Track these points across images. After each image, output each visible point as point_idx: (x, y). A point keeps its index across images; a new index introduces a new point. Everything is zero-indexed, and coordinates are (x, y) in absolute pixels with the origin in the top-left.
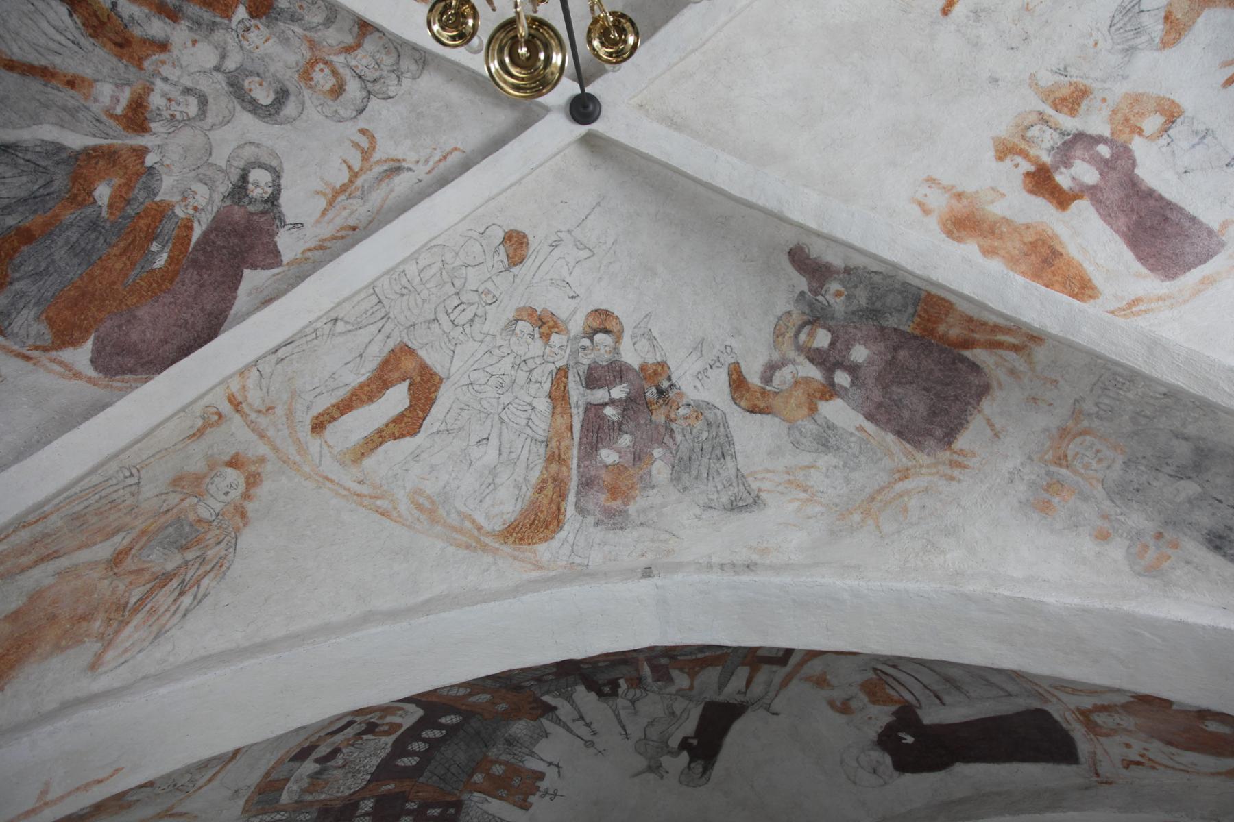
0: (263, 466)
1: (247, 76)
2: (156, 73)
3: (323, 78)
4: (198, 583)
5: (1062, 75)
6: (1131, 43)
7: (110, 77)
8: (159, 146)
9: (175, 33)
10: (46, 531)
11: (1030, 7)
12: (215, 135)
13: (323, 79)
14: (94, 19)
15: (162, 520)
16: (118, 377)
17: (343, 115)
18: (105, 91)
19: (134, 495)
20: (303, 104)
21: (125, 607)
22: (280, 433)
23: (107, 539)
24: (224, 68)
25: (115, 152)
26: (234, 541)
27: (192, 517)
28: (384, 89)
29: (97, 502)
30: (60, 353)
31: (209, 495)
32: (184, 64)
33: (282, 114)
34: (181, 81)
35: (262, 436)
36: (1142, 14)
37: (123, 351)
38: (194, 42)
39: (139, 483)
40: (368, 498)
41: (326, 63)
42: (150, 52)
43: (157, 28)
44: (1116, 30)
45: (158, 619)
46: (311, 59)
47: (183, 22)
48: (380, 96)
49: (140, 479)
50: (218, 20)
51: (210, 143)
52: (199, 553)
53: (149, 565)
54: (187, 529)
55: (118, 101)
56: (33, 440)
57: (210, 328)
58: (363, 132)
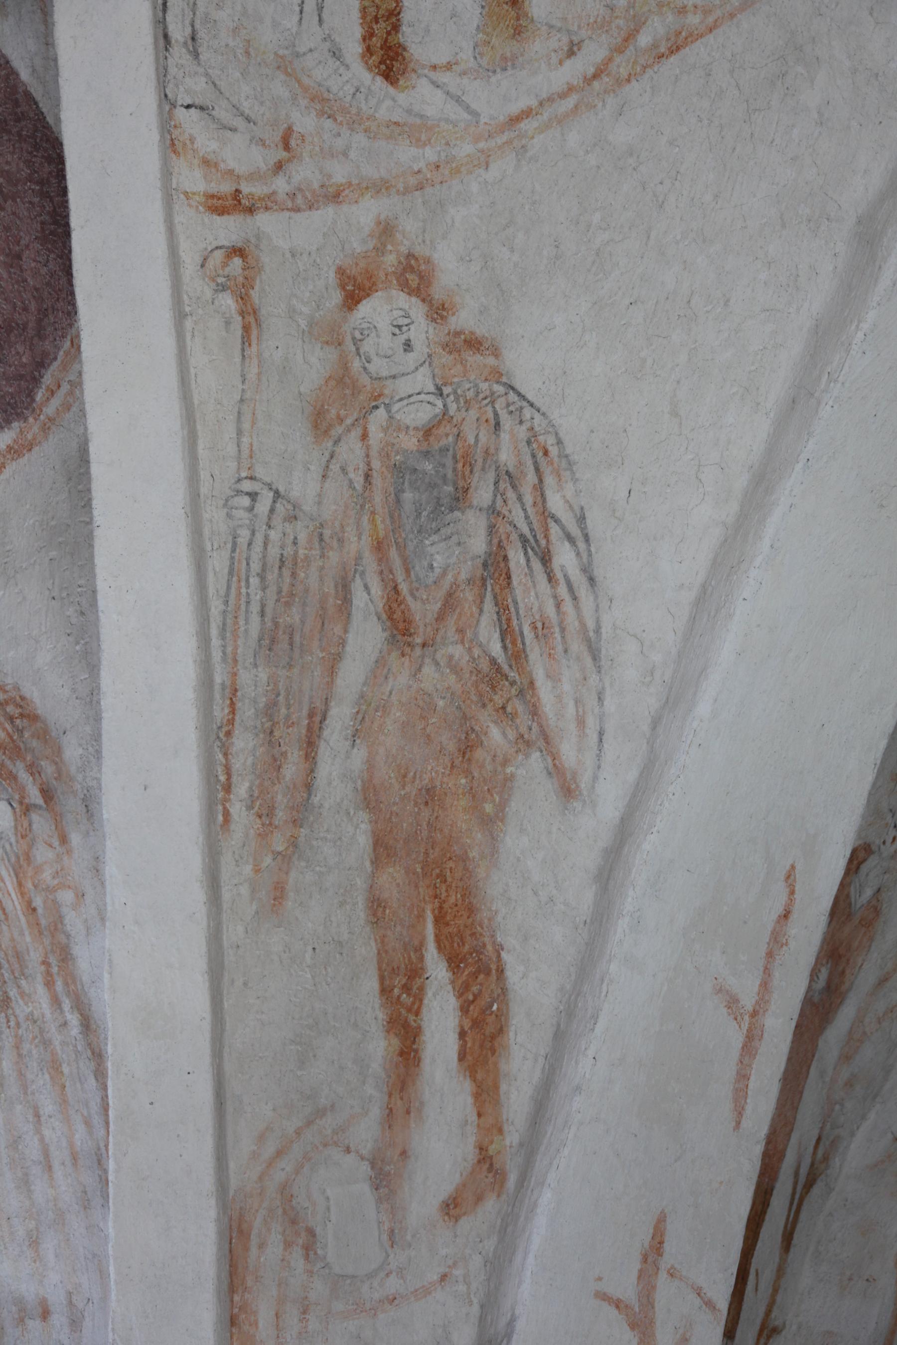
0: (399, 236)
4: (546, 516)
10: (261, 705)
15: (378, 498)
16: (39, 396)
19: (296, 518)
21: (499, 670)
22: (352, 155)
26: (512, 396)
27: (410, 443)
29: (264, 589)
31: (389, 382)
35: (335, 197)
39: (277, 493)
40: (618, 59)
45: (563, 630)
49: (269, 486)
52: (491, 476)
53: (449, 578)
54: (428, 467)
56: (74, 620)
57: (36, 147)
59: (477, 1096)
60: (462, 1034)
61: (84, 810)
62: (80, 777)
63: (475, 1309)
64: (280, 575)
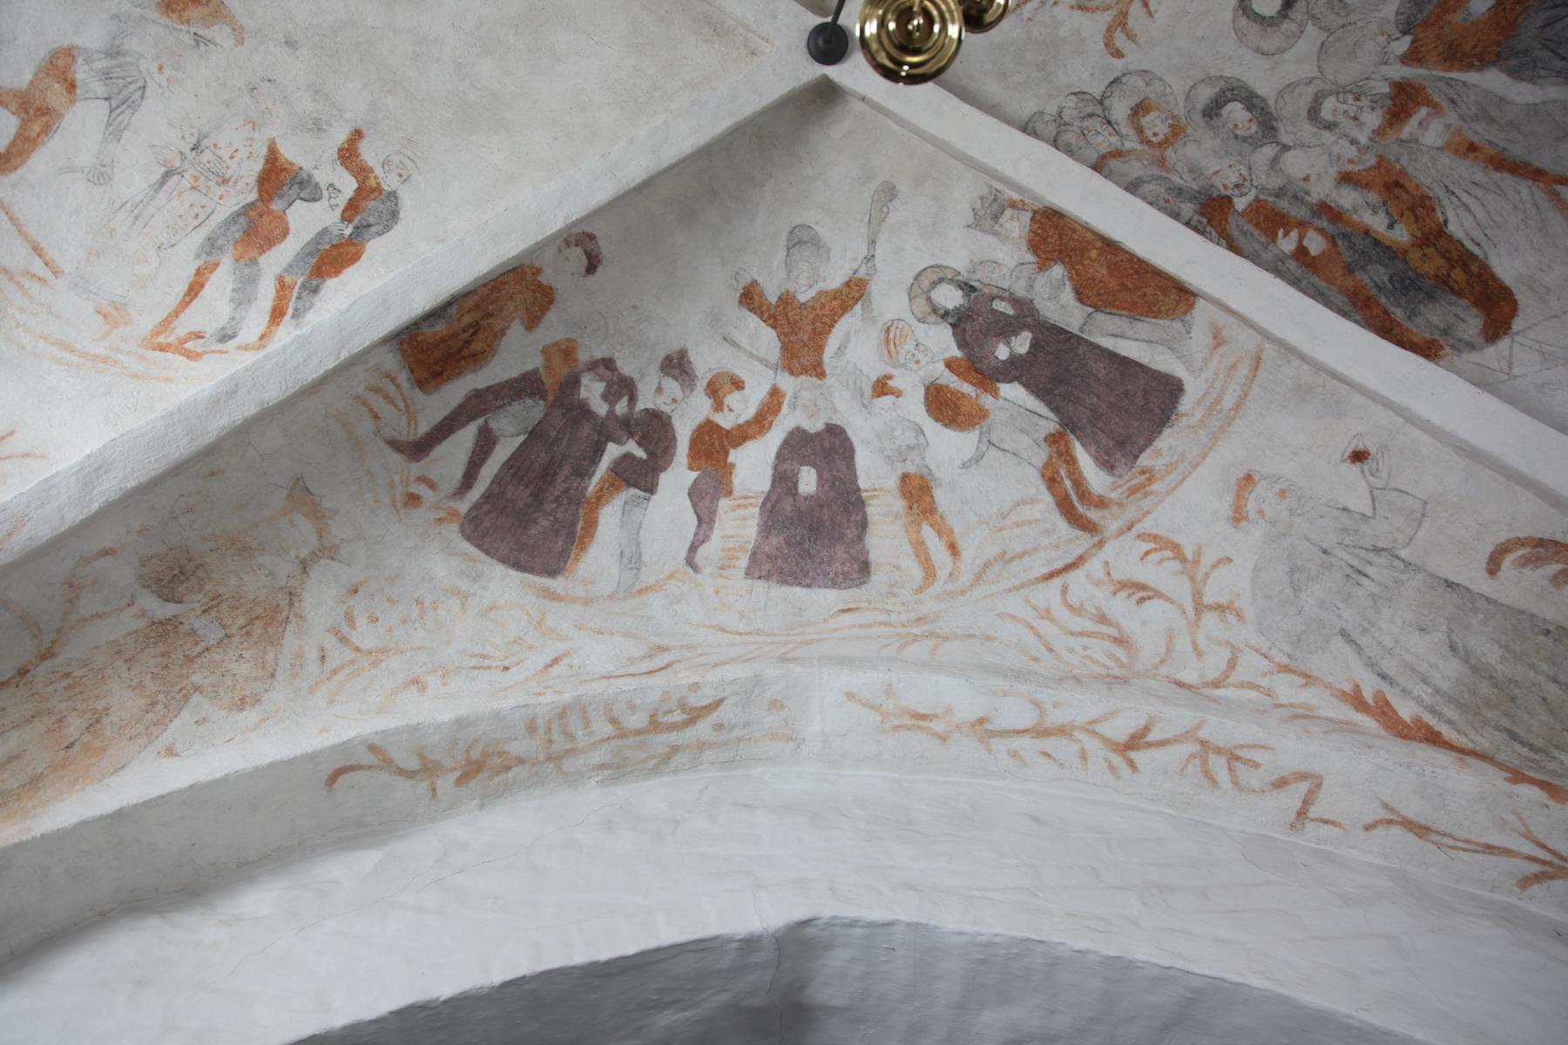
1: (1251, 137)
2: (1363, 150)
3: (1155, 126)
5: (201, 37)
6: (114, 62)
7: (1421, 151)
8: (1386, 63)
9: (1327, 191)
11: (250, 126)
12: (1310, 70)
13: (1156, 125)
14: (1419, 214)
17: (1138, 78)
18: (1434, 135)
20: (1188, 98)
24: (1277, 149)
25: (1445, 60)
28: (1081, 105)
32: (1325, 157)
33: (1217, 89)
34: (1334, 138)
36: (106, 96)
38: (1307, 179)
41: (1149, 142)
42: (1365, 174)
43: (1347, 199)
44: (136, 81)
46: (1166, 148)
47: (1314, 201)
48: (1088, 97)
50: (1271, 199)
51: (1319, 61)
55: (1420, 123)
58: (1118, 54)
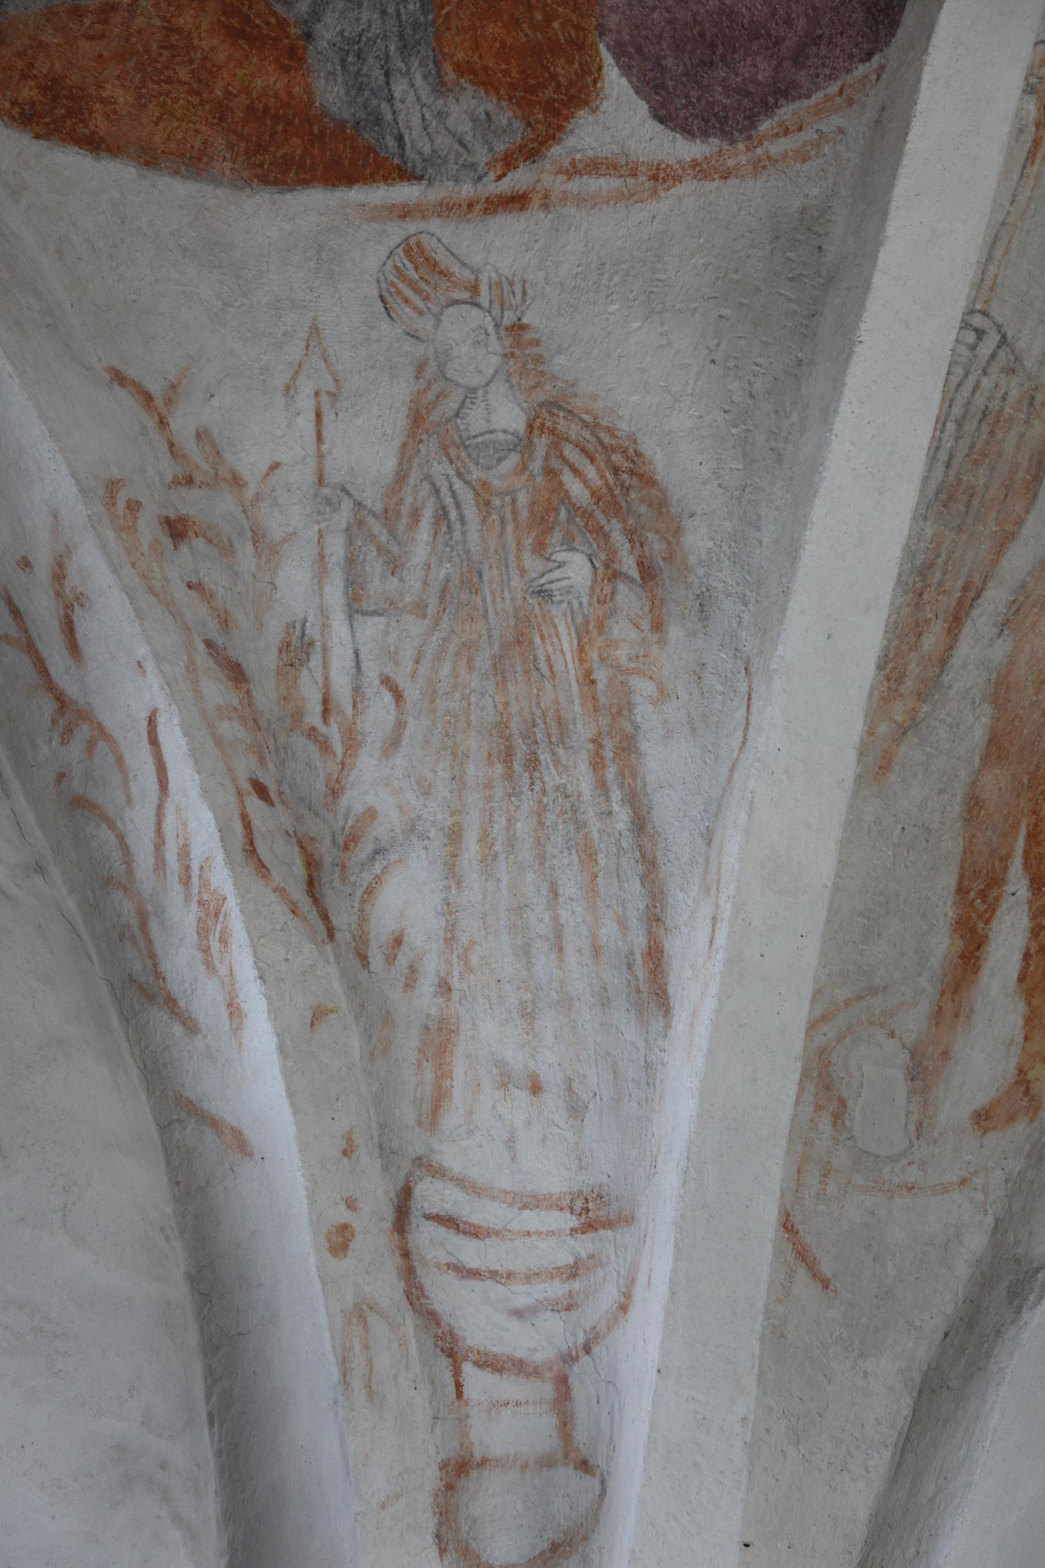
10: (918, 562)
16: (765, 126)
19: (1014, 371)
23: (1034, 497)
29: (957, 438)
30: (570, 141)
37: (713, 46)
39: (1004, 337)
49: (999, 327)
56: (737, 398)
59: (1029, 1020)
60: (1027, 956)
61: (697, 607)
62: (701, 571)
63: (990, 1220)
64: (978, 429)
